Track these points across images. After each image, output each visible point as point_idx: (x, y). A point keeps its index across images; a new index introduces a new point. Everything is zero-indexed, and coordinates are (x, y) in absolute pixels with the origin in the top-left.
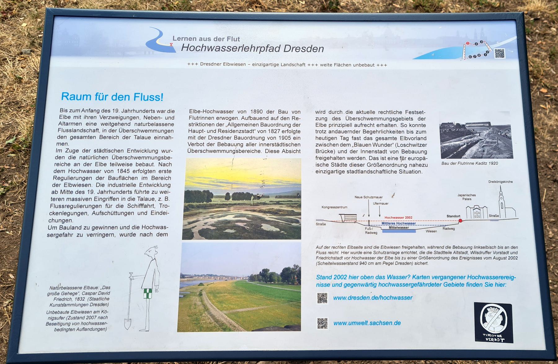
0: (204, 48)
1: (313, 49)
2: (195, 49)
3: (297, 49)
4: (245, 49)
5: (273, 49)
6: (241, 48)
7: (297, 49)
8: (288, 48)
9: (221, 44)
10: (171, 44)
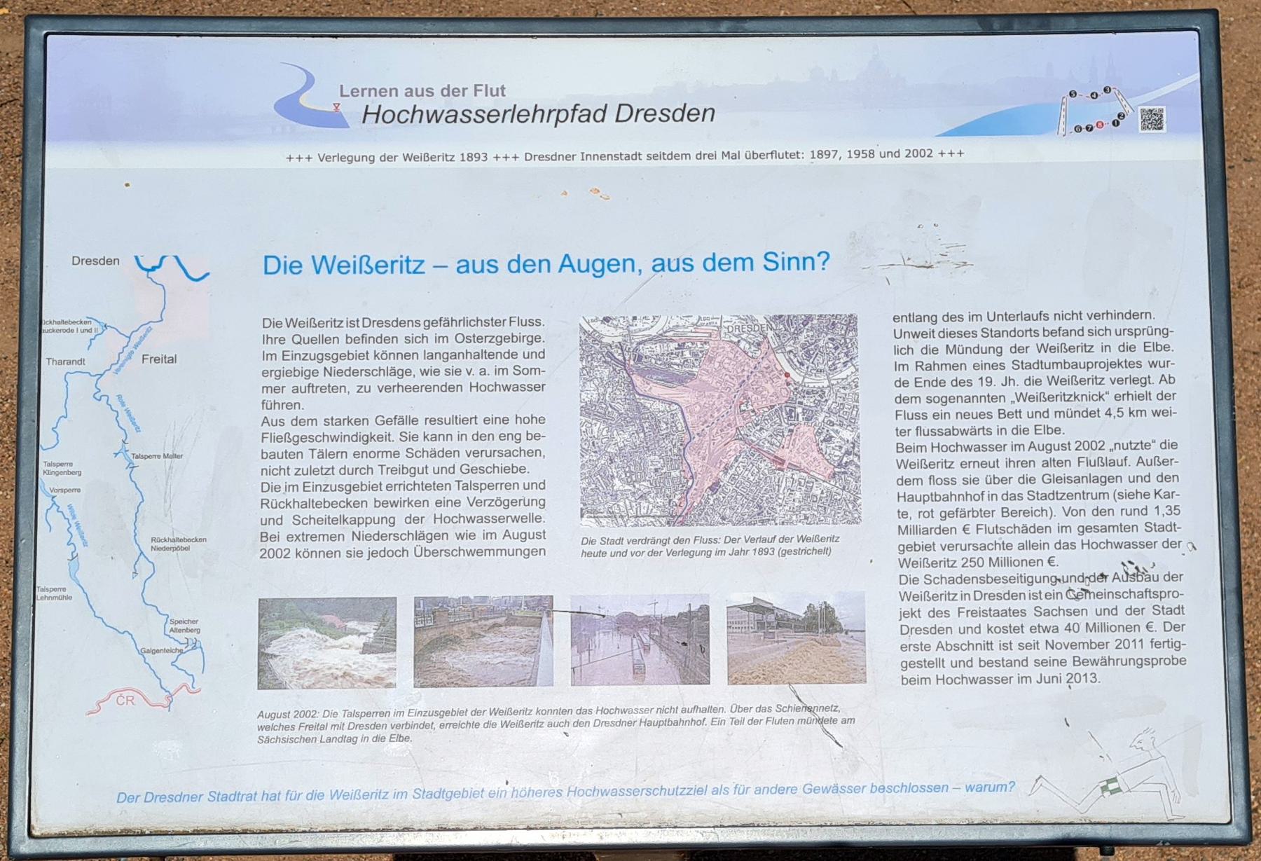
0: (418, 115)
1: (688, 114)
3: (649, 115)
4: (518, 115)
5: (588, 116)
6: (509, 114)
7: (649, 115)
8: (625, 113)
9: (459, 104)
10: (337, 105)
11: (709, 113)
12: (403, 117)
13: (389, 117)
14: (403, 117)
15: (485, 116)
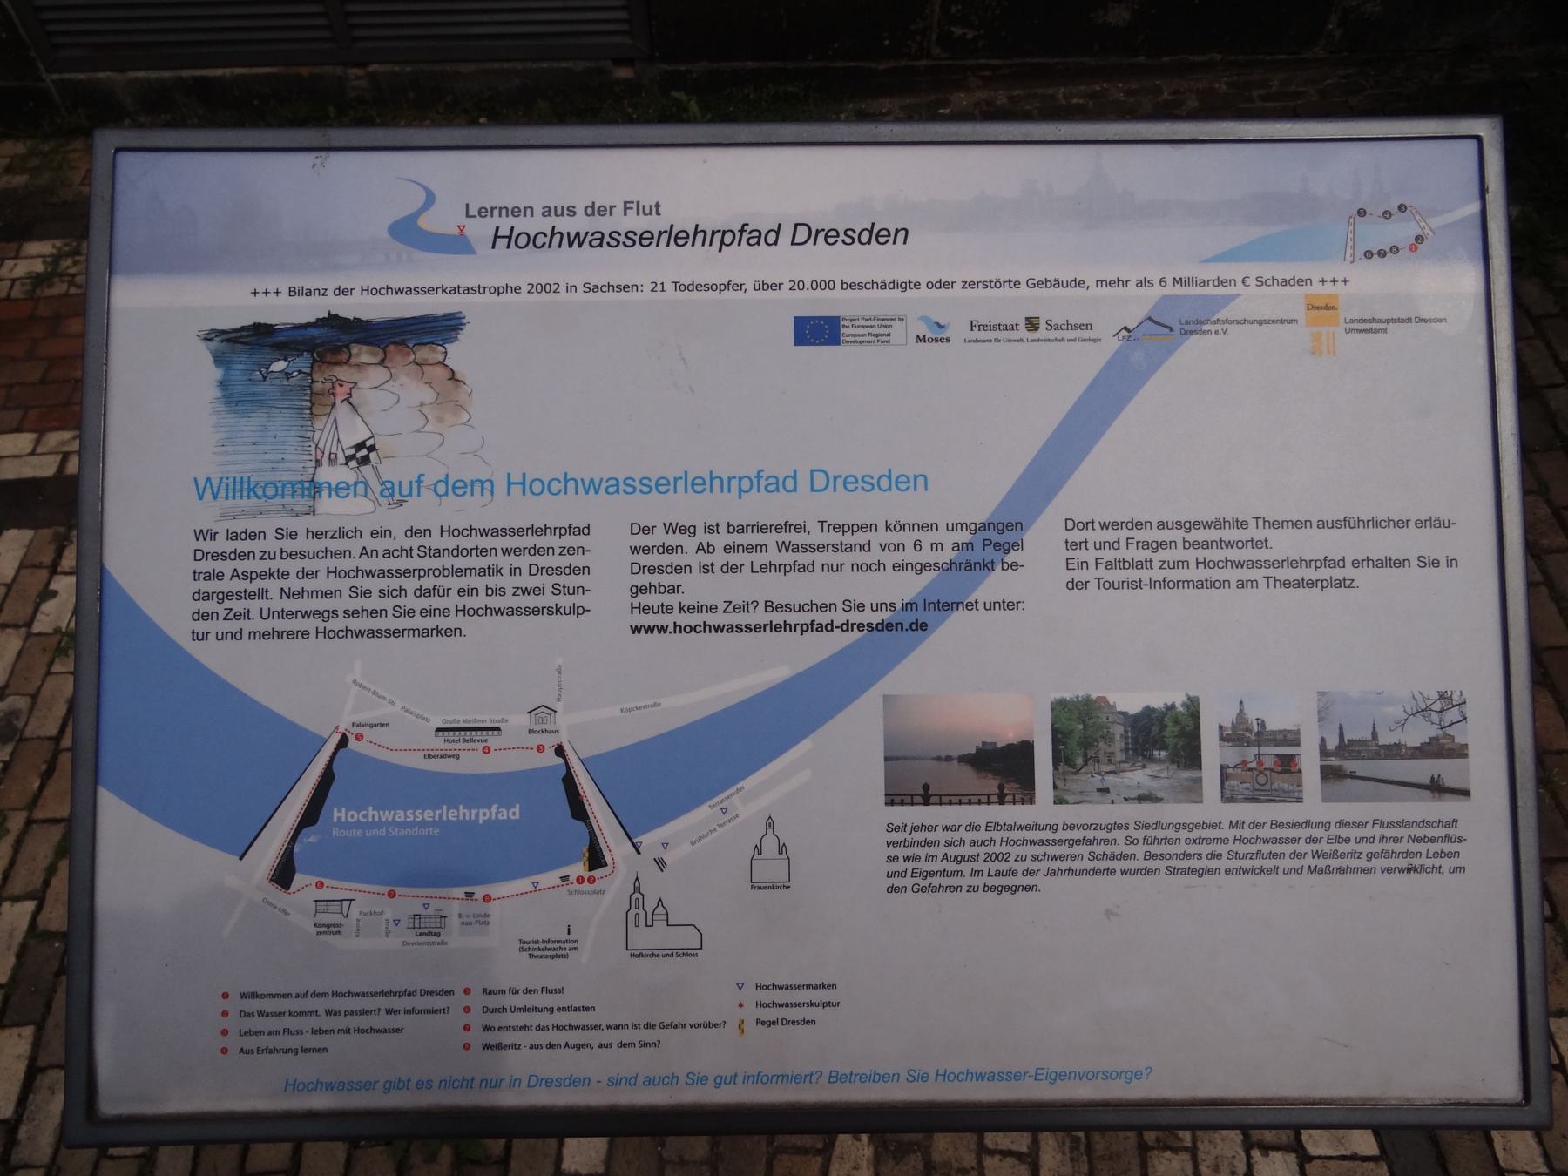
1: (877, 235)
2: (532, 241)
3: (830, 236)
4: (677, 237)
5: (758, 238)
6: (665, 236)
7: (830, 236)
8: (802, 234)
9: (605, 224)
10: (461, 228)
11: (901, 235)
12: (540, 240)
13: (522, 241)
14: (540, 240)
15: (637, 238)
